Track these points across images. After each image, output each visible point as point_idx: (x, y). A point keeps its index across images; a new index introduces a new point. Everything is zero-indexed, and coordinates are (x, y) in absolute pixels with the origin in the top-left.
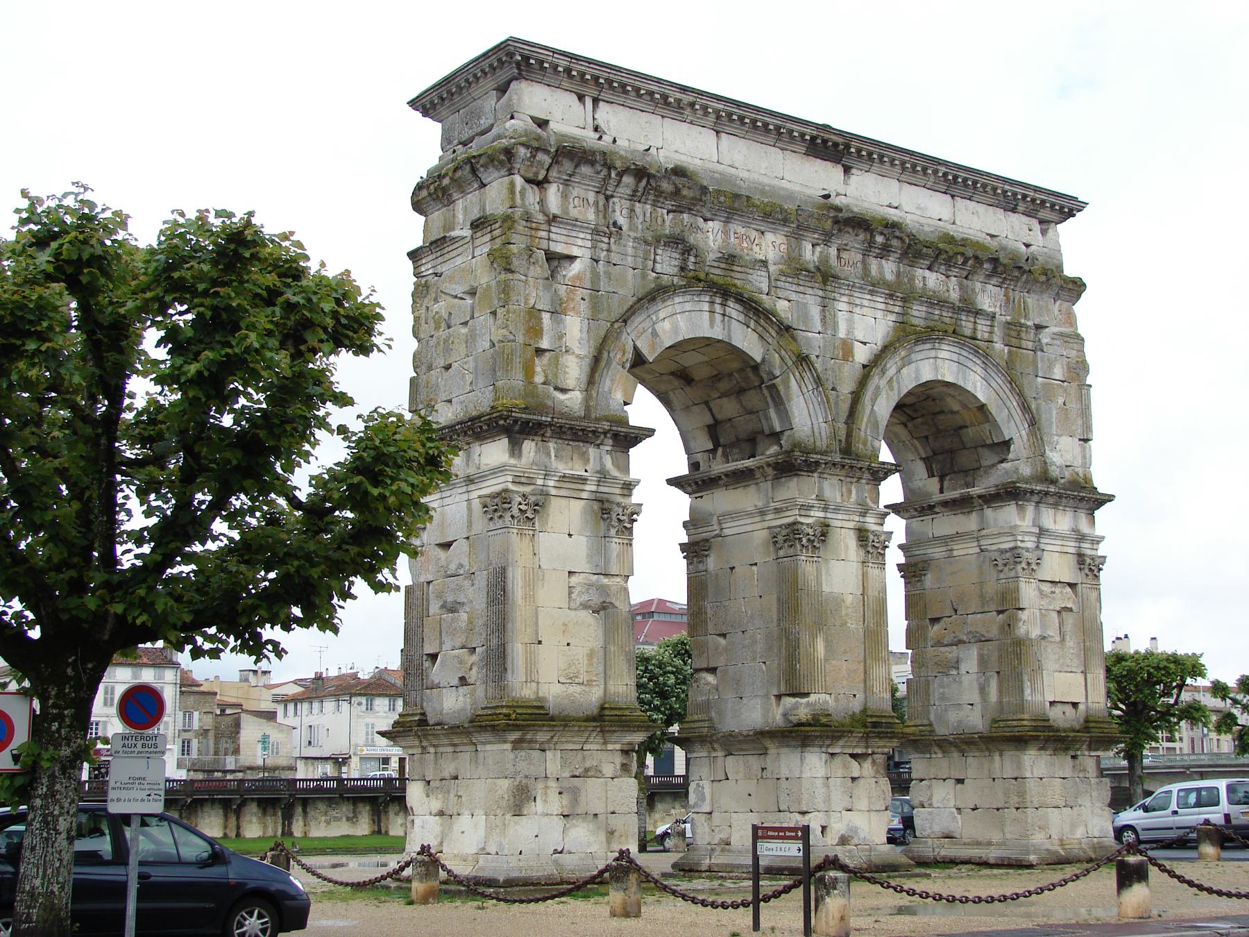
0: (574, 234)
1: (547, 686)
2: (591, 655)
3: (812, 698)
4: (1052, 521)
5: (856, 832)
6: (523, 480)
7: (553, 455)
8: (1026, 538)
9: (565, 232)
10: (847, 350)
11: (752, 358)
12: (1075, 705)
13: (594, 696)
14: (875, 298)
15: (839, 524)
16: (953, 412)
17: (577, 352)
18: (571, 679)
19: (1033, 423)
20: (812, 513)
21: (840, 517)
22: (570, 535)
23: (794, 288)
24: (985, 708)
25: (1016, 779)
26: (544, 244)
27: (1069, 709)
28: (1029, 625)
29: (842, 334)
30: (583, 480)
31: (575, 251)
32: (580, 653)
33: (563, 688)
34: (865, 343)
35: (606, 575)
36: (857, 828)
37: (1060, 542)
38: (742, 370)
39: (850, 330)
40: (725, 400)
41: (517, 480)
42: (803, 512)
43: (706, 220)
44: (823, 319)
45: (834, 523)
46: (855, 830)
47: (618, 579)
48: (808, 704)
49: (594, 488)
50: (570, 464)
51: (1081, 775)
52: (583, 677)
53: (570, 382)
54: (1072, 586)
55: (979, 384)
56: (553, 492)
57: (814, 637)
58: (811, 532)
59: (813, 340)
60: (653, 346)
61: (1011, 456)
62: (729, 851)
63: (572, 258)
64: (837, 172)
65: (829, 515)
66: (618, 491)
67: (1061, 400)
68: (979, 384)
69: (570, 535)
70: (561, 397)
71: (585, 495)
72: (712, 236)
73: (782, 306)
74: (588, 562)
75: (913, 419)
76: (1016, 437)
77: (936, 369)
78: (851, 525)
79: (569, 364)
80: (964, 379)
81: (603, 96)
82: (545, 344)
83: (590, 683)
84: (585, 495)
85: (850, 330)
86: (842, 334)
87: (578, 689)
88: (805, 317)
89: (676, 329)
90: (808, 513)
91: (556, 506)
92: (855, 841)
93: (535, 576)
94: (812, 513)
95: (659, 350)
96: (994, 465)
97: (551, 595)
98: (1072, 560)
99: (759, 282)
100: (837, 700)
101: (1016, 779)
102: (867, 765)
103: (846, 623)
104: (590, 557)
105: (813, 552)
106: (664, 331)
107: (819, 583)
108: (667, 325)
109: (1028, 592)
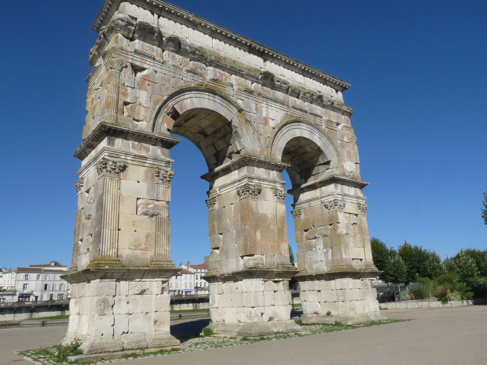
0: (145, 59)
1: (122, 250)
2: (148, 236)
3: (255, 256)
4: (347, 191)
5: (277, 315)
6: (114, 155)
7: (131, 147)
8: (339, 196)
9: (141, 57)
10: (266, 121)
11: (228, 120)
12: (361, 260)
13: (150, 254)
14: (276, 104)
16: (308, 152)
17: (145, 105)
18: (137, 247)
19: (338, 155)
20: (254, 181)
21: (265, 183)
22: (138, 182)
23: (244, 95)
24: (327, 261)
25: (341, 289)
26: (130, 61)
27: (359, 261)
28: (342, 229)
29: (264, 115)
30: (146, 158)
31: (146, 66)
33: (132, 251)
34: (273, 120)
35: (157, 201)
36: (277, 313)
37: (351, 199)
38: (224, 126)
39: (267, 114)
40: (220, 141)
41: (111, 155)
42: (250, 180)
43: (207, 66)
44: (256, 109)
45: (263, 186)
46: (276, 314)
47: (163, 202)
48: (254, 259)
49: (152, 162)
51: (366, 287)
52: (143, 246)
53: (141, 117)
54: (356, 215)
55: (317, 140)
56: (130, 162)
57: (255, 231)
58: (253, 188)
59: (252, 116)
61: (331, 167)
62: (224, 324)
64: (261, 60)
66: (163, 164)
67: (347, 149)
68: (317, 140)
69: (138, 182)
70: (137, 123)
71: (147, 165)
72: (210, 72)
73: (239, 102)
74: (147, 194)
75: (294, 157)
76: (332, 160)
77: (301, 133)
78: (270, 187)
79: (141, 110)
80: (312, 137)
81: (162, 14)
82: (128, 100)
83: (146, 249)
84: (147, 165)
85: (267, 114)
86: (264, 115)
87: (140, 252)
88: (250, 107)
89: (192, 103)
90: (252, 181)
91: (131, 169)
92: (276, 319)
93: (119, 199)
94: (254, 181)
96: (324, 171)
97: (127, 209)
98: (356, 206)
99: (229, 91)
100: (266, 257)
101: (341, 289)
103: (269, 226)
104: (148, 192)
106: (187, 103)
107: (257, 209)
109: (341, 217)
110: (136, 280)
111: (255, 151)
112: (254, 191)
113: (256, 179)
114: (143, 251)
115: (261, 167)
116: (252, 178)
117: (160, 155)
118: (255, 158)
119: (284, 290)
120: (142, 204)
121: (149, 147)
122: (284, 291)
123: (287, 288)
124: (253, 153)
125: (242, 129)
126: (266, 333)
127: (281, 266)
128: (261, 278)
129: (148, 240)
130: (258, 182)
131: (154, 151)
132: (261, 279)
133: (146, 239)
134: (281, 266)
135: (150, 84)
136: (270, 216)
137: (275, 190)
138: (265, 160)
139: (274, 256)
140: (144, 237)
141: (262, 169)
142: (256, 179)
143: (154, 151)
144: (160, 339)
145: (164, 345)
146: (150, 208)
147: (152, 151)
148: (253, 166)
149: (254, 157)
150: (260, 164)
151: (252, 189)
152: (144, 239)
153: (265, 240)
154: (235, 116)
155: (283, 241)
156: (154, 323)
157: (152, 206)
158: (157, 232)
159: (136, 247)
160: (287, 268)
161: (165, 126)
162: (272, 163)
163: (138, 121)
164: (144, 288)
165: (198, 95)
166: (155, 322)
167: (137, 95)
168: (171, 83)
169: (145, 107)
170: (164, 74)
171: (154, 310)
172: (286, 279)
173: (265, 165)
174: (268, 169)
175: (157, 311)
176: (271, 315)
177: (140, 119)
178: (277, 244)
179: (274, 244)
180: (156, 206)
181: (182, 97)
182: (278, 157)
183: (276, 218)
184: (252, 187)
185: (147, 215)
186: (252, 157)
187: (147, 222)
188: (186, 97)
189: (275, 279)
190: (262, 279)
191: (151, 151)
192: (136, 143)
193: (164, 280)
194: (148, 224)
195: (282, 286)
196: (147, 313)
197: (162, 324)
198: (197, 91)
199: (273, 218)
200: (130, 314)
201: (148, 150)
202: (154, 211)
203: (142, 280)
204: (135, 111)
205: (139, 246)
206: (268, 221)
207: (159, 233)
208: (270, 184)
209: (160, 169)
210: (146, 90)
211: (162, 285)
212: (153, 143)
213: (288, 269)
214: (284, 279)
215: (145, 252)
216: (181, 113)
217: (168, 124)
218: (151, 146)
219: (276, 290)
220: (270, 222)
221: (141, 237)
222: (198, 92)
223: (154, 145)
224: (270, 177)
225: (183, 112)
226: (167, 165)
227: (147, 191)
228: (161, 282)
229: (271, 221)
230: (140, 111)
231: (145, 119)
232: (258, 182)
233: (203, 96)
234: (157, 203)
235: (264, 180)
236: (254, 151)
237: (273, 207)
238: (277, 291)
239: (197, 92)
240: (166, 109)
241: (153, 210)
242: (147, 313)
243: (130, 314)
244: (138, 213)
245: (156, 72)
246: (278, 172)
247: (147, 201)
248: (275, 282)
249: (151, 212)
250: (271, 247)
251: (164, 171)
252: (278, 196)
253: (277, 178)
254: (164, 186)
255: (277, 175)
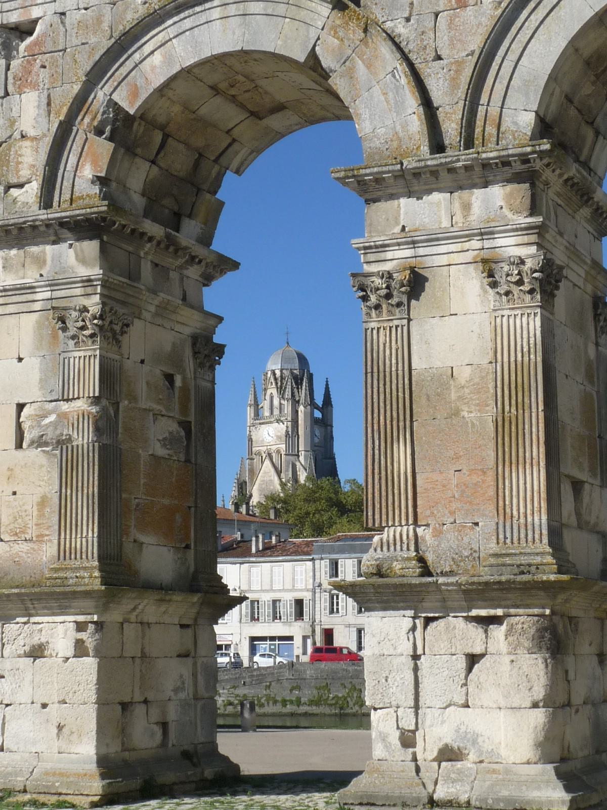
2: (43, 503)
5: (474, 742)
15: (444, 260)
20: (389, 255)
22: (20, 360)
30: (31, 289)
31: (35, 13)
32: (29, 501)
45: (429, 262)
49: (48, 295)
50: (21, 274)
52: (32, 532)
60: (135, 93)
63: (35, 22)
65: (421, 251)
66: (78, 291)
79: (23, 151)
84: (37, 306)
87: (25, 547)
89: (169, 60)
90: (382, 256)
92: (472, 757)
94: (389, 255)
95: (144, 96)
100: (437, 534)
102: (498, 632)
103: (457, 413)
105: (390, 312)
106: (153, 68)
108: (157, 58)
110: (18, 620)
111: (401, 135)
112: (383, 292)
113: (399, 244)
114: (31, 545)
115: (429, 192)
116: (376, 247)
117: (72, 268)
118: (376, 170)
119: (509, 653)
120: (29, 417)
121: (44, 252)
122: (513, 657)
123: (528, 644)
124: (395, 144)
125: (350, 75)
126: (387, 797)
127: (492, 561)
128: (405, 609)
129: (43, 515)
130: (408, 253)
131: (57, 258)
132: (402, 612)
133: (39, 511)
134: (492, 561)
135: (46, 64)
136: (464, 374)
137: (489, 267)
138: (422, 164)
139: (477, 524)
140: (35, 508)
141: (436, 196)
142: (399, 244)
143: (57, 258)
144: (54, 774)
145: (60, 791)
146: (48, 426)
147: (52, 261)
148: (392, 197)
149: (368, 171)
150: (415, 182)
151: (378, 289)
152: (35, 513)
153: (433, 471)
154: (324, 35)
155: (518, 462)
156: (56, 731)
157: (52, 418)
158: (64, 491)
159: (16, 534)
160: (516, 571)
161: (87, 172)
162: (460, 164)
163: (21, 186)
164: (36, 641)
165: (187, 24)
166: (60, 728)
167: (15, 114)
168: (105, 26)
169: (34, 139)
170: (86, 9)
171: (56, 701)
172: (521, 611)
173: (437, 178)
174: (461, 188)
175: (64, 702)
176: (448, 740)
177: (22, 180)
178: (490, 478)
179: (475, 478)
180: (63, 416)
181: (137, 57)
182: (515, 123)
183: (492, 376)
184: (378, 281)
185: (46, 444)
186: (362, 172)
187: (41, 466)
188: (147, 49)
189: (474, 612)
190: (411, 613)
191: (49, 262)
192: (14, 252)
193: (81, 618)
194: (44, 469)
195: (503, 638)
196: (44, 706)
197: (75, 735)
198: (183, 11)
199: (477, 380)
200: (7, 705)
201: (40, 261)
202: (58, 432)
203: (33, 620)
204: (9, 161)
205: (23, 532)
206: (453, 396)
207: (69, 492)
208: (467, 246)
209: (65, 309)
210: (35, 86)
211: (74, 633)
212: (53, 238)
213: (522, 573)
214: (512, 611)
215: (36, 547)
216: (132, 112)
217: (95, 163)
218: (49, 249)
219: (478, 650)
220: (460, 398)
221: (28, 507)
222: (187, 13)
223: (54, 243)
224: (472, 218)
225: (139, 103)
226: (89, 290)
227: (41, 379)
228: (72, 626)
229: (467, 391)
230: (20, 156)
231: (32, 174)
232: (408, 253)
233: (203, 18)
234: (65, 407)
235: (433, 239)
236: (400, 140)
237: (480, 336)
238: (482, 656)
239: (182, 15)
240: (87, 120)
241: (56, 428)
242: (44, 706)
243: (7, 705)
244: (25, 445)
245: (63, 14)
246: (510, 188)
247: (41, 408)
248: (479, 620)
249: (51, 435)
250: (463, 492)
251: (75, 310)
252: (502, 289)
253: (506, 211)
254: (82, 354)
255: (509, 197)
